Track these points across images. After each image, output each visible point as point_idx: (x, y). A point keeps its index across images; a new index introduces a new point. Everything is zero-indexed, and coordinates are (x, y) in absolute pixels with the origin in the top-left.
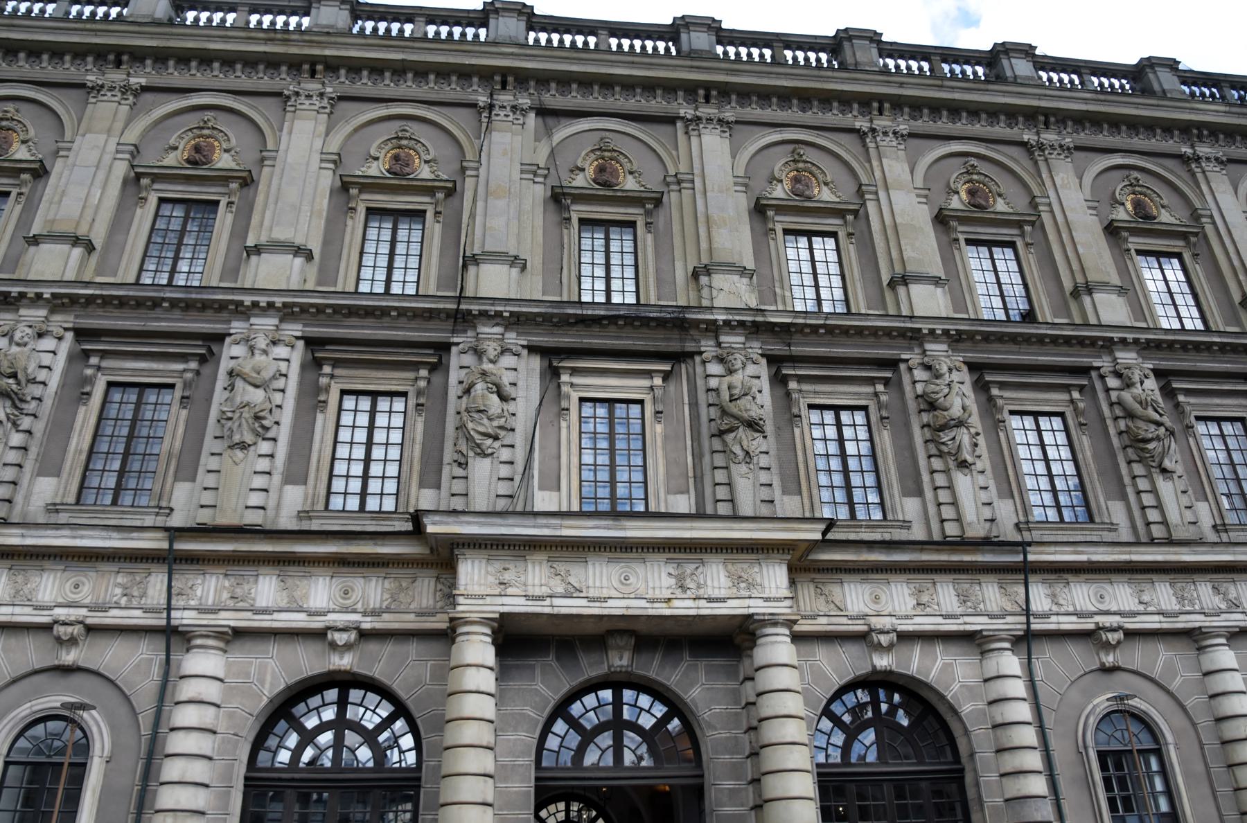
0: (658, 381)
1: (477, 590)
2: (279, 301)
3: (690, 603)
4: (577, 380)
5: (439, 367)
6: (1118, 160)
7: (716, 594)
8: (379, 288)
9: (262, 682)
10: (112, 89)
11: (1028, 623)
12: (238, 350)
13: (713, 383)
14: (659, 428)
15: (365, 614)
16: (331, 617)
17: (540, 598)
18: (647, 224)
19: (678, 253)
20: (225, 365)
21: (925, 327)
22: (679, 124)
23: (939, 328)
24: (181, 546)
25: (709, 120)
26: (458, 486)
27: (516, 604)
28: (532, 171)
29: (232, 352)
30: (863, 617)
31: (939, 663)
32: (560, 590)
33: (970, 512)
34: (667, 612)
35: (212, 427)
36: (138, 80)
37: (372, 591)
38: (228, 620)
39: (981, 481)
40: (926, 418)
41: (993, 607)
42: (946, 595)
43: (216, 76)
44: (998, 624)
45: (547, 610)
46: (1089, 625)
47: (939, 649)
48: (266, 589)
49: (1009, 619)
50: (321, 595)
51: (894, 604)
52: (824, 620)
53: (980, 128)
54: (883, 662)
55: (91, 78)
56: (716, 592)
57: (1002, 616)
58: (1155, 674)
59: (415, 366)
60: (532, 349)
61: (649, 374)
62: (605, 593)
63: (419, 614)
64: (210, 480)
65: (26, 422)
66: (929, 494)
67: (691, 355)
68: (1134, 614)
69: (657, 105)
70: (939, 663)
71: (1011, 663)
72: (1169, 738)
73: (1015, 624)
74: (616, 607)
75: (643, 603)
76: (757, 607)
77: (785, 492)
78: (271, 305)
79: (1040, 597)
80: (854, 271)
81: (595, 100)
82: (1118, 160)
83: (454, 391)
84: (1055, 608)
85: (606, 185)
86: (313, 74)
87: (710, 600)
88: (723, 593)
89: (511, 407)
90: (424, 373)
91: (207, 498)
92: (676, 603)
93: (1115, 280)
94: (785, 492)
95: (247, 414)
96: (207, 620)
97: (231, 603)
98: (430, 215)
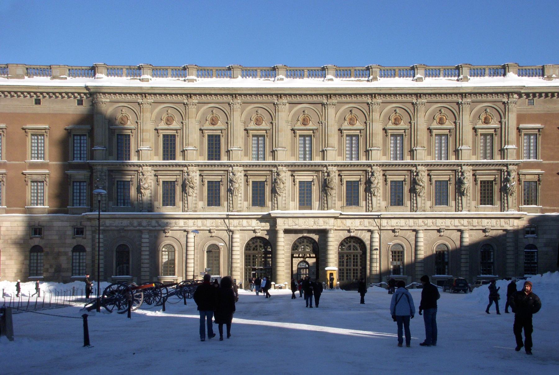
13: (325, 178)
27: (287, 227)
28: (287, 122)
39: (378, 198)
47: (364, 231)
54: (352, 234)
55: (185, 101)
65: (195, 192)
72: (405, 249)
74: (303, 227)
76: (327, 227)
77: (339, 201)
79: (384, 222)
82: (439, 105)
85: (305, 125)
89: (285, 185)
94: (339, 201)
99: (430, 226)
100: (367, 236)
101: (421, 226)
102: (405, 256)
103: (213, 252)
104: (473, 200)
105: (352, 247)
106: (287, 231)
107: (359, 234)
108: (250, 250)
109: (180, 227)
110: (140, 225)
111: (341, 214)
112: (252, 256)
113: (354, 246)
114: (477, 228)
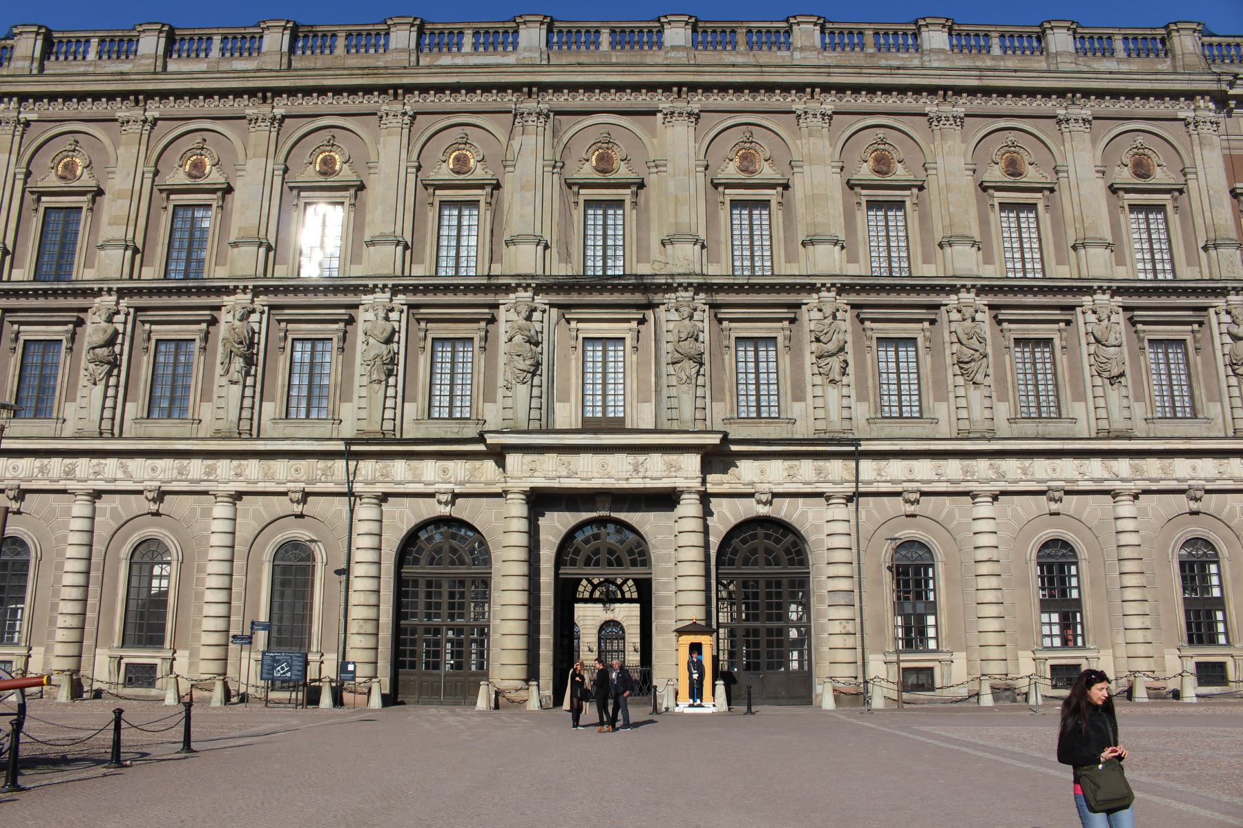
0: (634, 324)
1: (516, 474)
2: (390, 283)
3: (640, 480)
4: (581, 325)
5: (492, 320)
6: (1002, 123)
7: (655, 475)
8: (451, 272)
9: (402, 522)
10: (264, 120)
11: (857, 487)
12: (370, 316)
13: (671, 326)
14: (635, 357)
15: (456, 484)
16: (437, 486)
17: (553, 478)
18: (635, 204)
19: (654, 225)
20: (360, 326)
21: (818, 282)
22: (659, 115)
23: (828, 282)
24: (354, 448)
25: (680, 114)
26: (509, 402)
27: (540, 482)
29: (362, 315)
30: (753, 483)
31: (799, 511)
32: (565, 474)
33: (834, 415)
34: (626, 486)
35: (359, 369)
36: (279, 112)
37: (459, 470)
38: (380, 488)
39: (845, 391)
40: (815, 346)
41: (837, 478)
42: (807, 468)
43: (328, 103)
44: (839, 488)
45: (557, 485)
46: (898, 488)
48: (399, 468)
49: (846, 485)
50: (430, 473)
51: (775, 474)
52: (727, 486)
53: (892, 102)
55: (248, 111)
56: (655, 472)
57: (842, 483)
58: (940, 519)
59: (477, 321)
60: (552, 305)
61: (628, 321)
62: (590, 475)
63: (487, 484)
64: (364, 403)
66: (809, 397)
67: (657, 305)
68: (930, 482)
69: (641, 100)
70: (799, 511)
71: (840, 511)
72: (939, 556)
73: (849, 488)
74: (597, 483)
75: (612, 481)
76: (680, 483)
78: (385, 286)
79: (868, 468)
80: (779, 233)
81: (597, 100)
82: (1002, 123)
83: (503, 338)
84: (878, 478)
85: (604, 171)
86: (396, 95)
87: (652, 479)
88: (659, 475)
90: (483, 324)
91: (363, 414)
92: (632, 481)
93: (975, 233)
95: (378, 362)
96: (369, 489)
97: (381, 479)
98: (482, 204)
99: (1016, 482)
100: (811, 516)
101: (988, 481)
102: (942, 583)
103: (293, 569)
104: (1137, 400)
105: (761, 555)
106: (541, 501)
107: (782, 510)
108: (416, 561)
109: (192, 481)
110: (69, 474)
111: (726, 439)
112: (422, 583)
113: (768, 551)
114: (1163, 485)
